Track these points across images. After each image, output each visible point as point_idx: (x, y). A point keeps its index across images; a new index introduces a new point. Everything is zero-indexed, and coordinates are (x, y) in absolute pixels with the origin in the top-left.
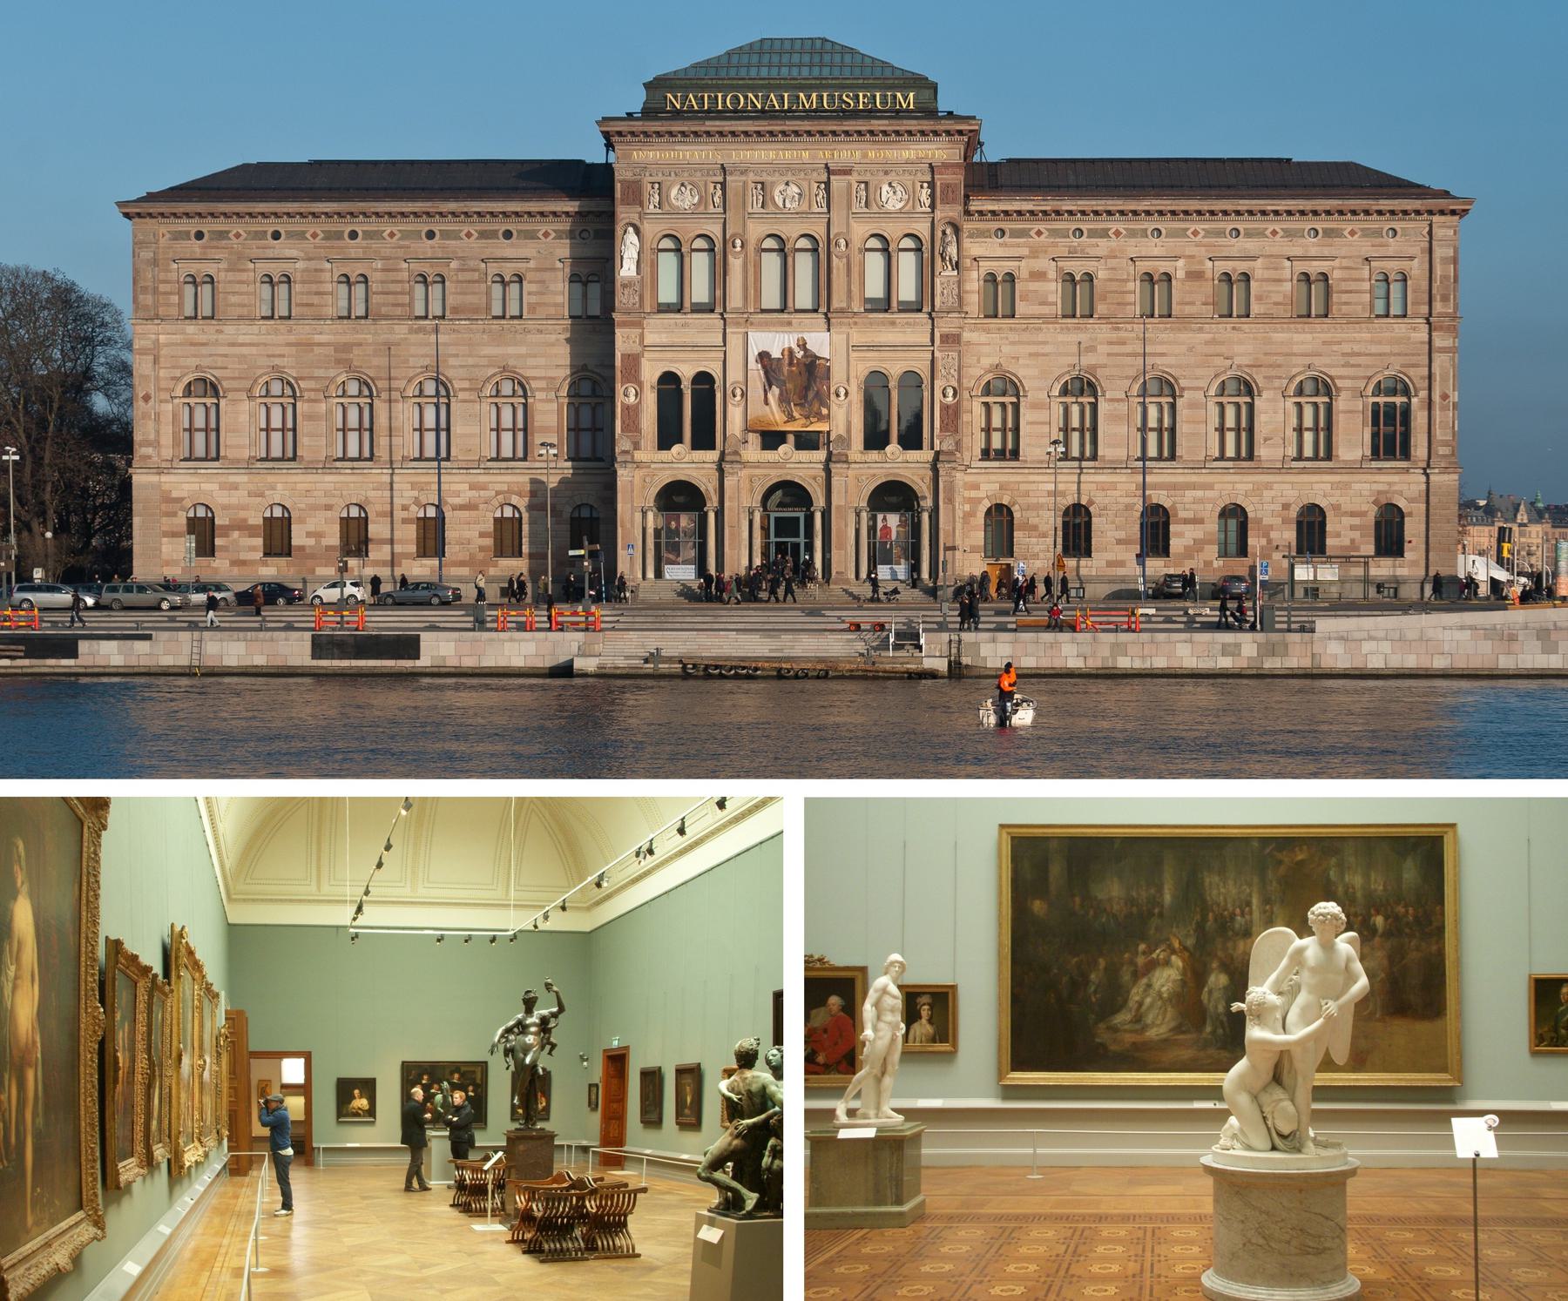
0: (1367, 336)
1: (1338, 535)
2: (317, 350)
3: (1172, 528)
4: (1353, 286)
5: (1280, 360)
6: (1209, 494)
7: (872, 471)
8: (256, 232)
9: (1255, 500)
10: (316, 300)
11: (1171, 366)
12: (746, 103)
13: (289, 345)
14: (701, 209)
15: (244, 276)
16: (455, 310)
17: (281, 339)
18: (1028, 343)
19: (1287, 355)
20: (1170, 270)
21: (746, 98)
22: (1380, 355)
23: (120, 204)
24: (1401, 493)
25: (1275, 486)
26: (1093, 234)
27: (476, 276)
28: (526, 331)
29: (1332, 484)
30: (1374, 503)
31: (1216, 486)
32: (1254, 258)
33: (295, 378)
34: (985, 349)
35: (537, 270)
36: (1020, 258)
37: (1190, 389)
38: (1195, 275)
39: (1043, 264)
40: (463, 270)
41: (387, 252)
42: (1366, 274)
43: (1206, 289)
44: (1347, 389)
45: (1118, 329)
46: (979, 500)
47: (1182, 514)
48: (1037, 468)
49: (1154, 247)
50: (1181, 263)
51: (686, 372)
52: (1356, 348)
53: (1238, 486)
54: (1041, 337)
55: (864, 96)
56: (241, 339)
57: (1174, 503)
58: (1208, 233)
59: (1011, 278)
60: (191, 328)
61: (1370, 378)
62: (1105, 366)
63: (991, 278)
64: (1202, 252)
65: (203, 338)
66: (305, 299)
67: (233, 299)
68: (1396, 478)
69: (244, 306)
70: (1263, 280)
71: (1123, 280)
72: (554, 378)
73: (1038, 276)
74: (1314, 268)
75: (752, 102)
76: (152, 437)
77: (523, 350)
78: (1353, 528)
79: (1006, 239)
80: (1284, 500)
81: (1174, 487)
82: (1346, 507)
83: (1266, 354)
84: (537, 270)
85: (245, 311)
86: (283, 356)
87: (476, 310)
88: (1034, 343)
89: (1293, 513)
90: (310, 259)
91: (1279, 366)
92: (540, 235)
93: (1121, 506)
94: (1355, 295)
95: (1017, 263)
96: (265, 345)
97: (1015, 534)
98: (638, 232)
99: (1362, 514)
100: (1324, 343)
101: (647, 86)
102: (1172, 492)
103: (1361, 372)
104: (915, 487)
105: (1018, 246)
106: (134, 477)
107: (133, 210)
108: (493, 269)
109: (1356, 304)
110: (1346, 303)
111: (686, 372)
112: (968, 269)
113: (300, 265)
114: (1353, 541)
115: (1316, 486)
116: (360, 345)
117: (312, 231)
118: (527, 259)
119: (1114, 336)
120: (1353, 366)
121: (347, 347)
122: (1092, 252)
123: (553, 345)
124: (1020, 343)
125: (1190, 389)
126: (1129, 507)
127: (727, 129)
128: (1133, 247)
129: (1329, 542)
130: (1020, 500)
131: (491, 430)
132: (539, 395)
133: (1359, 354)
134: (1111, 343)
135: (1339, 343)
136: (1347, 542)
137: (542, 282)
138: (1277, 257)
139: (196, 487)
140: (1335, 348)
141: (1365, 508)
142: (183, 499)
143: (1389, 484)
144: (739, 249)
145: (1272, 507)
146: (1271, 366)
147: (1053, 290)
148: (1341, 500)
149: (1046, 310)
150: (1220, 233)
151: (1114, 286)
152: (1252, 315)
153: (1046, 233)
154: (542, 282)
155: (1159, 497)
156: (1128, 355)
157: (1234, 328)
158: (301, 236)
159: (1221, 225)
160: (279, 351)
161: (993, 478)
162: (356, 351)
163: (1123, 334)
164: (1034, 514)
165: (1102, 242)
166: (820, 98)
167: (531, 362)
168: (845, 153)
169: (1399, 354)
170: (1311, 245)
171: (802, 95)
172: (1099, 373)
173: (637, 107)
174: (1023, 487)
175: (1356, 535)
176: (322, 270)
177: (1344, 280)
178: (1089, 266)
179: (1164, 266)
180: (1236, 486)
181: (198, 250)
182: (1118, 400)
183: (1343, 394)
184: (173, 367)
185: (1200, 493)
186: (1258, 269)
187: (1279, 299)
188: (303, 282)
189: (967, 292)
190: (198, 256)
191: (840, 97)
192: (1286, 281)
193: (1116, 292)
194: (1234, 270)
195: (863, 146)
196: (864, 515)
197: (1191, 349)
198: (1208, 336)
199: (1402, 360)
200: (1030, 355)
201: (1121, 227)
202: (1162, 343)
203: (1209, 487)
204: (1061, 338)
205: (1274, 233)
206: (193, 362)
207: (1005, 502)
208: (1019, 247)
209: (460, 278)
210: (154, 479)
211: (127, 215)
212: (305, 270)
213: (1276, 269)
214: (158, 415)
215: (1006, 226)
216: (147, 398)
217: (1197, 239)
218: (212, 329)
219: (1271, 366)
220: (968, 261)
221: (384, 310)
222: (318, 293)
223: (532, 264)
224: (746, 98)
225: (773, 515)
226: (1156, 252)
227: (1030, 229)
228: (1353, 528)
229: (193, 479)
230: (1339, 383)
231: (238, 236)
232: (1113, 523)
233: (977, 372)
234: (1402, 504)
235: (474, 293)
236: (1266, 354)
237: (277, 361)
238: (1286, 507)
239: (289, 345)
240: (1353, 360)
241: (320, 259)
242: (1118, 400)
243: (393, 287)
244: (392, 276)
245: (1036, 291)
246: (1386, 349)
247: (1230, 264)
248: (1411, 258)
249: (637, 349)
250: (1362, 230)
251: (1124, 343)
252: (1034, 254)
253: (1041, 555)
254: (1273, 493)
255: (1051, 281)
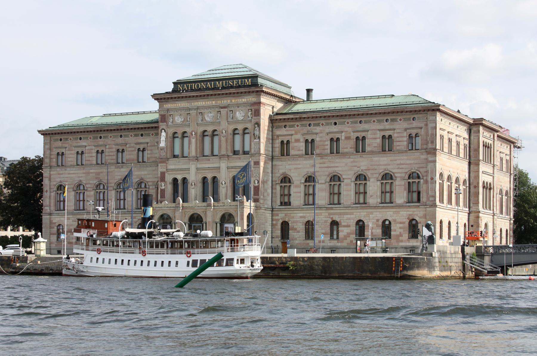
0: (406, 157)
1: (395, 231)
2: (91, 175)
3: (340, 229)
4: (401, 139)
5: (376, 167)
6: (352, 216)
7: (220, 210)
8: (76, 138)
9: (367, 218)
10: (90, 159)
11: (340, 171)
12: (201, 87)
13: (83, 173)
14: (184, 123)
15: (72, 152)
16: (127, 160)
17: (81, 171)
18: (294, 164)
19: (378, 165)
20: (340, 137)
21: (201, 85)
22: (410, 164)
23: (39, 131)
24: (417, 215)
25: (374, 213)
26: (315, 125)
27: (133, 149)
28: (147, 167)
29: (393, 212)
30: (408, 218)
31: (354, 214)
32: (368, 131)
33: (85, 184)
34: (281, 167)
35: (150, 146)
36: (292, 135)
37: (346, 179)
38: (348, 138)
39: (298, 136)
40: (130, 147)
41: (109, 142)
42: (405, 134)
43: (352, 142)
44: (399, 177)
45: (322, 158)
46: (278, 220)
47: (343, 224)
48: (298, 208)
49: (334, 129)
50: (343, 134)
51: (179, 177)
52: (402, 162)
53: (361, 213)
54: (298, 162)
55: (236, 81)
56: (71, 172)
57: (341, 220)
58: (352, 122)
59: (288, 142)
60: (58, 169)
61: (406, 173)
62: (318, 172)
63: (282, 142)
64: (350, 130)
65: (61, 172)
66: (88, 159)
67: (69, 159)
68: (415, 209)
69: (72, 161)
70: (371, 139)
71: (324, 141)
72: (154, 182)
73: (297, 141)
74: (387, 134)
75: (203, 86)
76: (48, 203)
77: (146, 173)
78: (400, 228)
79: (287, 128)
80: (377, 218)
81: (340, 214)
82: (399, 219)
83: (371, 165)
84: (150, 146)
85: (72, 163)
86: (82, 177)
87: (133, 160)
88: (296, 164)
89: (380, 223)
90: (89, 146)
91: (376, 169)
92: (151, 135)
93: (323, 221)
94: (401, 142)
95: (291, 137)
96: (77, 173)
97: (290, 231)
98: (165, 131)
99: (403, 223)
100: (391, 160)
101: (174, 83)
102: (340, 216)
103: (404, 171)
104: (233, 215)
105: (291, 130)
106: (43, 217)
107: (44, 133)
108: (138, 147)
109: (402, 146)
110: (398, 146)
111: (179, 177)
112: (276, 140)
113: (87, 148)
114: (400, 233)
115: (388, 213)
116: (102, 172)
117: (90, 137)
118: (148, 143)
119: (321, 161)
120: (401, 168)
121: (98, 174)
122: (314, 131)
123: (154, 171)
124: (292, 164)
125: (346, 179)
126: (326, 222)
127: (188, 95)
128: (329, 129)
129: (392, 233)
130: (291, 219)
131: (138, 199)
132: (151, 187)
133: (403, 164)
134: (320, 163)
135: (396, 160)
136: (398, 233)
137: (151, 150)
138: (375, 130)
139: (59, 219)
140: (395, 162)
141: (404, 220)
142: (56, 223)
143: (413, 211)
144: (194, 136)
145: (373, 221)
146: (373, 169)
147: (302, 145)
148: (397, 218)
149: (300, 153)
150: (356, 122)
151: (321, 143)
152: (366, 151)
153: (300, 126)
154: (151, 150)
155: (337, 218)
156: (326, 167)
157: (360, 156)
158: (87, 138)
159: (356, 119)
160: (81, 175)
161: (283, 212)
162: (101, 174)
163: (324, 160)
164: (296, 224)
165: (318, 128)
166: (223, 83)
167: (148, 176)
168: (226, 101)
169: (417, 164)
170: (387, 125)
171: (217, 82)
172: (317, 174)
173: (170, 90)
174: (292, 215)
175: (402, 230)
176: (92, 149)
177: (398, 137)
178: (313, 137)
179: (337, 136)
180: (361, 214)
181: (60, 144)
182: (323, 184)
183: (398, 179)
184: (54, 182)
185: (349, 216)
186: (369, 135)
187: (376, 145)
188: (87, 153)
189: (275, 147)
190: (60, 146)
191: (229, 82)
192: (378, 138)
193: (321, 145)
194: (361, 135)
195: (230, 98)
196: (218, 225)
197: (346, 165)
198: (352, 160)
199: (418, 166)
200: (295, 168)
201: (323, 122)
202: (337, 163)
203: (352, 214)
204: (304, 162)
205: (374, 121)
206: (59, 180)
207: (286, 220)
208: (291, 131)
209: (129, 150)
210: (48, 217)
211: (42, 134)
212: (88, 149)
213: (375, 134)
214: (50, 197)
215: (287, 124)
216: (47, 191)
217: (348, 125)
218: (64, 169)
219: (373, 169)
220: (276, 137)
221: (109, 161)
222: (91, 157)
223: (149, 145)
224: (201, 85)
225: (193, 225)
226: (335, 130)
227: (295, 125)
228: (400, 228)
229: (59, 217)
230: (396, 175)
231: (71, 139)
232: (321, 227)
233: (278, 175)
234: (417, 219)
235: (133, 155)
236: (371, 165)
237: (80, 179)
238: (378, 220)
239: (83, 173)
240: (401, 166)
241: (91, 145)
242: (323, 184)
243: (111, 154)
244: (111, 150)
245: (297, 146)
246: (412, 162)
247: (359, 133)
248: (421, 128)
249: (165, 170)
250: (404, 119)
251: (324, 163)
252: (296, 134)
253: (298, 239)
254: (373, 216)
255: (301, 142)
